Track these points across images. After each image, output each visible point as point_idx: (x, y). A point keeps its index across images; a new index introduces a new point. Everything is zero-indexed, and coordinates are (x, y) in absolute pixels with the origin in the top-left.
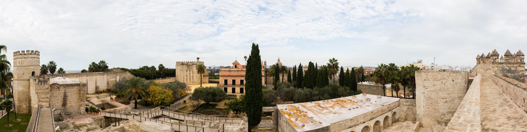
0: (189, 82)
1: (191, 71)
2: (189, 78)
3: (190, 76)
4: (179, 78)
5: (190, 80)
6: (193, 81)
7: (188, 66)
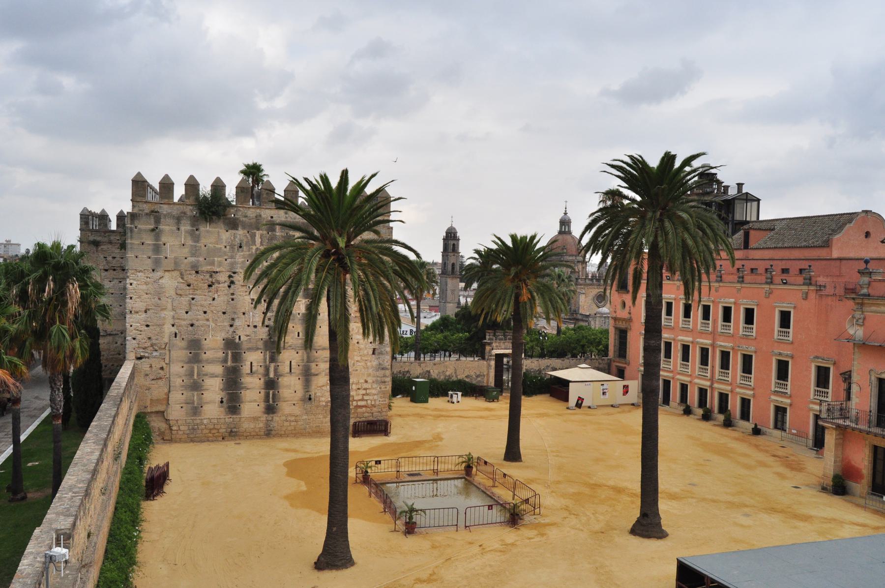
0: (297, 410)
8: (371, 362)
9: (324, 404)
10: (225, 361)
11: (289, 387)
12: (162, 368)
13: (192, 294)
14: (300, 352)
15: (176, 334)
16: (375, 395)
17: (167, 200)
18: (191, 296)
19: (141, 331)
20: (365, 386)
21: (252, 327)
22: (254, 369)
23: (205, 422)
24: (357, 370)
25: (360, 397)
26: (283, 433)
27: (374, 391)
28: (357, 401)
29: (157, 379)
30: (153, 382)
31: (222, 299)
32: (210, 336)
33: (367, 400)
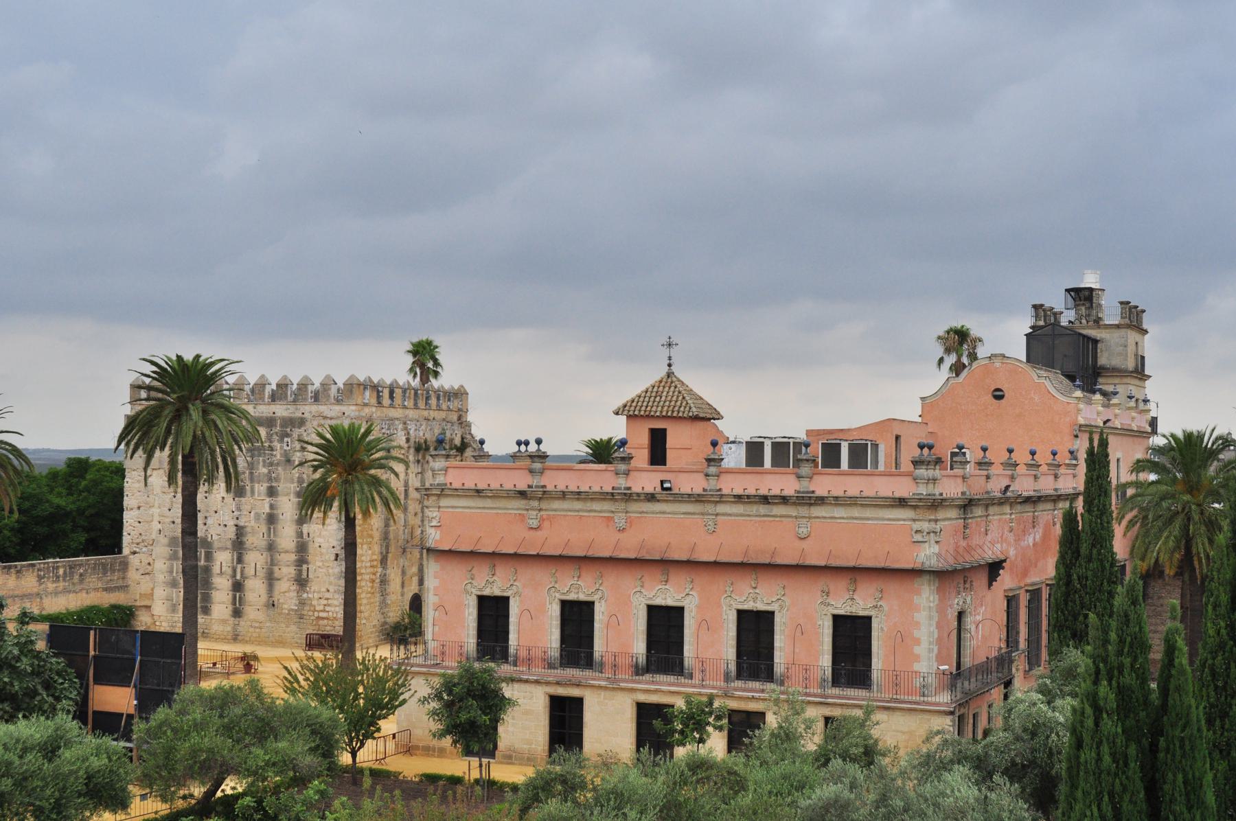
0: (261, 616)
2: (261, 573)
3: (271, 547)
8: (332, 568)
12: (149, 564)
14: (265, 554)
16: (336, 606)
20: (327, 595)
21: (222, 526)
22: (224, 569)
24: (318, 577)
25: (321, 608)
28: (318, 611)
29: (146, 574)
30: (143, 577)
33: (328, 612)
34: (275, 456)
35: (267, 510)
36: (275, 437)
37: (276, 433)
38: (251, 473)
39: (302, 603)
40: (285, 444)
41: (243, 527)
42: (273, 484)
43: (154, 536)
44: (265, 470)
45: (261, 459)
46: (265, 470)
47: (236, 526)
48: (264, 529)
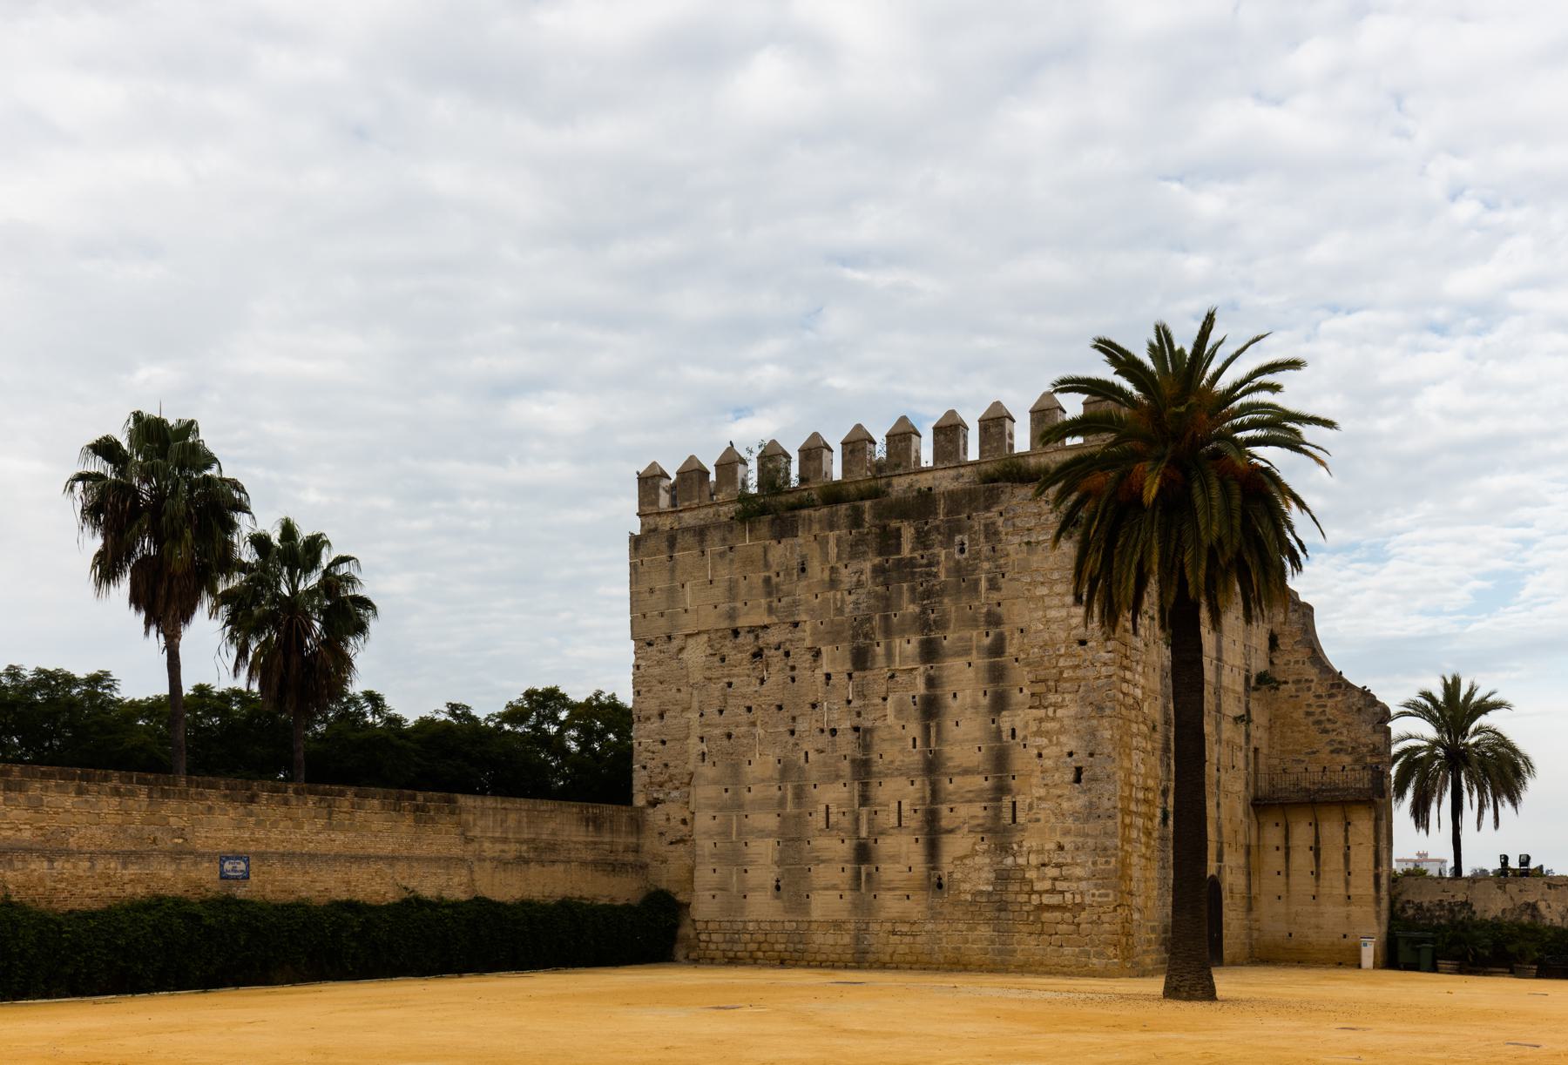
0: (915, 908)
1: (950, 639)
2: (913, 821)
3: (932, 766)
4: (704, 821)
5: (933, 851)
6: (1003, 877)
7: (888, 541)
8: (1069, 799)
9: (969, 897)
10: (782, 803)
11: (894, 858)
12: (684, 822)
13: (729, 676)
15: (703, 754)
16: (1080, 879)
17: (687, 504)
18: (726, 680)
19: (653, 753)
20: (1057, 859)
21: (827, 733)
22: (833, 819)
23: (751, 926)
24: (1038, 820)
25: (1047, 885)
26: (887, 958)
27: (1078, 872)
28: (1040, 893)
29: (677, 842)
30: (672, 847)
31: (776, 676)
32: (758, 755)
33: (1062, 892)
34: (936, 575)
35: (921, 688)
36: (935, 537)
37: (937, 528)
38: (886, 619)
39: (1003, 877)
40: (957, 548)
41: (869, 731)
42: (933, 635)
43: (690, 767)
44: (913, 609)
45: (905, 586)
46: (913, 609)
47: (856, 729)
48: (914, 729)
